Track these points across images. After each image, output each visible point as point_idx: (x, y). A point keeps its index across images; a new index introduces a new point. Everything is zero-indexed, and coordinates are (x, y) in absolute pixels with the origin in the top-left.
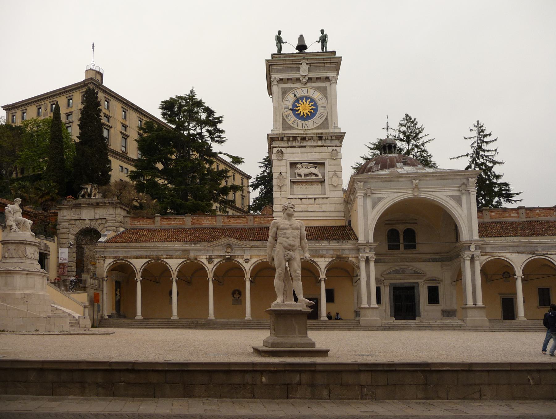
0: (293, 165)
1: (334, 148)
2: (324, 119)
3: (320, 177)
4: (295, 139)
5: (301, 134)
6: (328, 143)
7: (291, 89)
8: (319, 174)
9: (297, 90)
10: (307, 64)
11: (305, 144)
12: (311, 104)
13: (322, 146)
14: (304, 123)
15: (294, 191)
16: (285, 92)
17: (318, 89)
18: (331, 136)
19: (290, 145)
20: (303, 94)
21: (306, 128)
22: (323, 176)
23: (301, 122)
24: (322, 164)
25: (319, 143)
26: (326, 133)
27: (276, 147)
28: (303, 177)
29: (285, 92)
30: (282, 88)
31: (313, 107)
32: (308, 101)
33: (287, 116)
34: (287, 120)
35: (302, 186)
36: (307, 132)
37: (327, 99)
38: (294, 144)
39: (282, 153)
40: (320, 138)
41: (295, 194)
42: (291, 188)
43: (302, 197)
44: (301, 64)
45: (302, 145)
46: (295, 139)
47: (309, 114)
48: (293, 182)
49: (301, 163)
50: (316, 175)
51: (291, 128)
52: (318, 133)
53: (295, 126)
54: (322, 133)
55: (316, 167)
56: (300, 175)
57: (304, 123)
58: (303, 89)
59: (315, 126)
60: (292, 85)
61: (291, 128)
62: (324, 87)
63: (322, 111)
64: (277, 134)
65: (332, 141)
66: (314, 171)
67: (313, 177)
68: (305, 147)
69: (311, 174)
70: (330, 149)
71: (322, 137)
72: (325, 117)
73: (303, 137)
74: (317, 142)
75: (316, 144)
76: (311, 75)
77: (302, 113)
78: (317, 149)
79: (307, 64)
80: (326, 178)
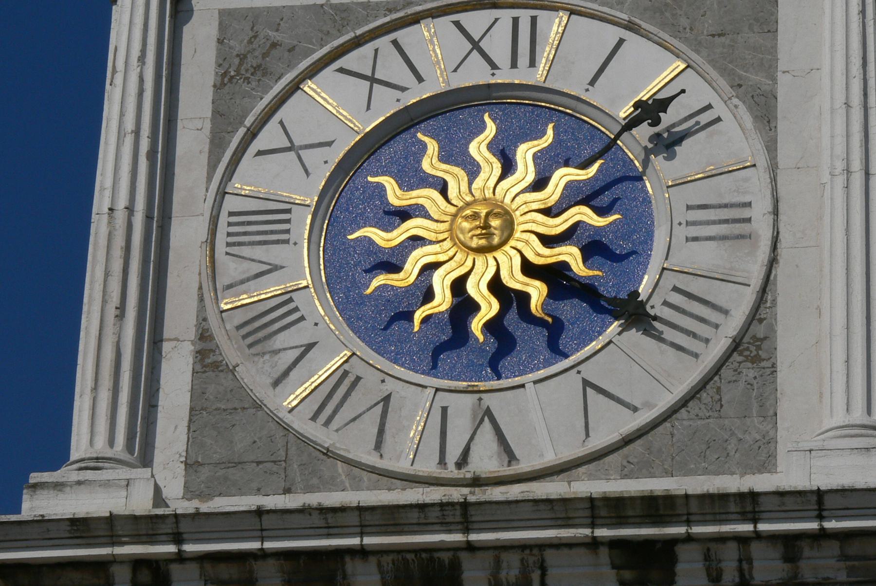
12: (563, 176)
14: (462, 407)
20: (476, 74)
26: (716, 505)
32: (525, 154)
33: (260, 328)
34: (254, 376)
37: (764, 110)
47: (537, 291)
52: (615, 508)
53: (357, 444)
54: (656, 508)
57: (462, 407)
59: (600, 439)
63: (707, 256)
72: (732, 326)
77: (441, 283)
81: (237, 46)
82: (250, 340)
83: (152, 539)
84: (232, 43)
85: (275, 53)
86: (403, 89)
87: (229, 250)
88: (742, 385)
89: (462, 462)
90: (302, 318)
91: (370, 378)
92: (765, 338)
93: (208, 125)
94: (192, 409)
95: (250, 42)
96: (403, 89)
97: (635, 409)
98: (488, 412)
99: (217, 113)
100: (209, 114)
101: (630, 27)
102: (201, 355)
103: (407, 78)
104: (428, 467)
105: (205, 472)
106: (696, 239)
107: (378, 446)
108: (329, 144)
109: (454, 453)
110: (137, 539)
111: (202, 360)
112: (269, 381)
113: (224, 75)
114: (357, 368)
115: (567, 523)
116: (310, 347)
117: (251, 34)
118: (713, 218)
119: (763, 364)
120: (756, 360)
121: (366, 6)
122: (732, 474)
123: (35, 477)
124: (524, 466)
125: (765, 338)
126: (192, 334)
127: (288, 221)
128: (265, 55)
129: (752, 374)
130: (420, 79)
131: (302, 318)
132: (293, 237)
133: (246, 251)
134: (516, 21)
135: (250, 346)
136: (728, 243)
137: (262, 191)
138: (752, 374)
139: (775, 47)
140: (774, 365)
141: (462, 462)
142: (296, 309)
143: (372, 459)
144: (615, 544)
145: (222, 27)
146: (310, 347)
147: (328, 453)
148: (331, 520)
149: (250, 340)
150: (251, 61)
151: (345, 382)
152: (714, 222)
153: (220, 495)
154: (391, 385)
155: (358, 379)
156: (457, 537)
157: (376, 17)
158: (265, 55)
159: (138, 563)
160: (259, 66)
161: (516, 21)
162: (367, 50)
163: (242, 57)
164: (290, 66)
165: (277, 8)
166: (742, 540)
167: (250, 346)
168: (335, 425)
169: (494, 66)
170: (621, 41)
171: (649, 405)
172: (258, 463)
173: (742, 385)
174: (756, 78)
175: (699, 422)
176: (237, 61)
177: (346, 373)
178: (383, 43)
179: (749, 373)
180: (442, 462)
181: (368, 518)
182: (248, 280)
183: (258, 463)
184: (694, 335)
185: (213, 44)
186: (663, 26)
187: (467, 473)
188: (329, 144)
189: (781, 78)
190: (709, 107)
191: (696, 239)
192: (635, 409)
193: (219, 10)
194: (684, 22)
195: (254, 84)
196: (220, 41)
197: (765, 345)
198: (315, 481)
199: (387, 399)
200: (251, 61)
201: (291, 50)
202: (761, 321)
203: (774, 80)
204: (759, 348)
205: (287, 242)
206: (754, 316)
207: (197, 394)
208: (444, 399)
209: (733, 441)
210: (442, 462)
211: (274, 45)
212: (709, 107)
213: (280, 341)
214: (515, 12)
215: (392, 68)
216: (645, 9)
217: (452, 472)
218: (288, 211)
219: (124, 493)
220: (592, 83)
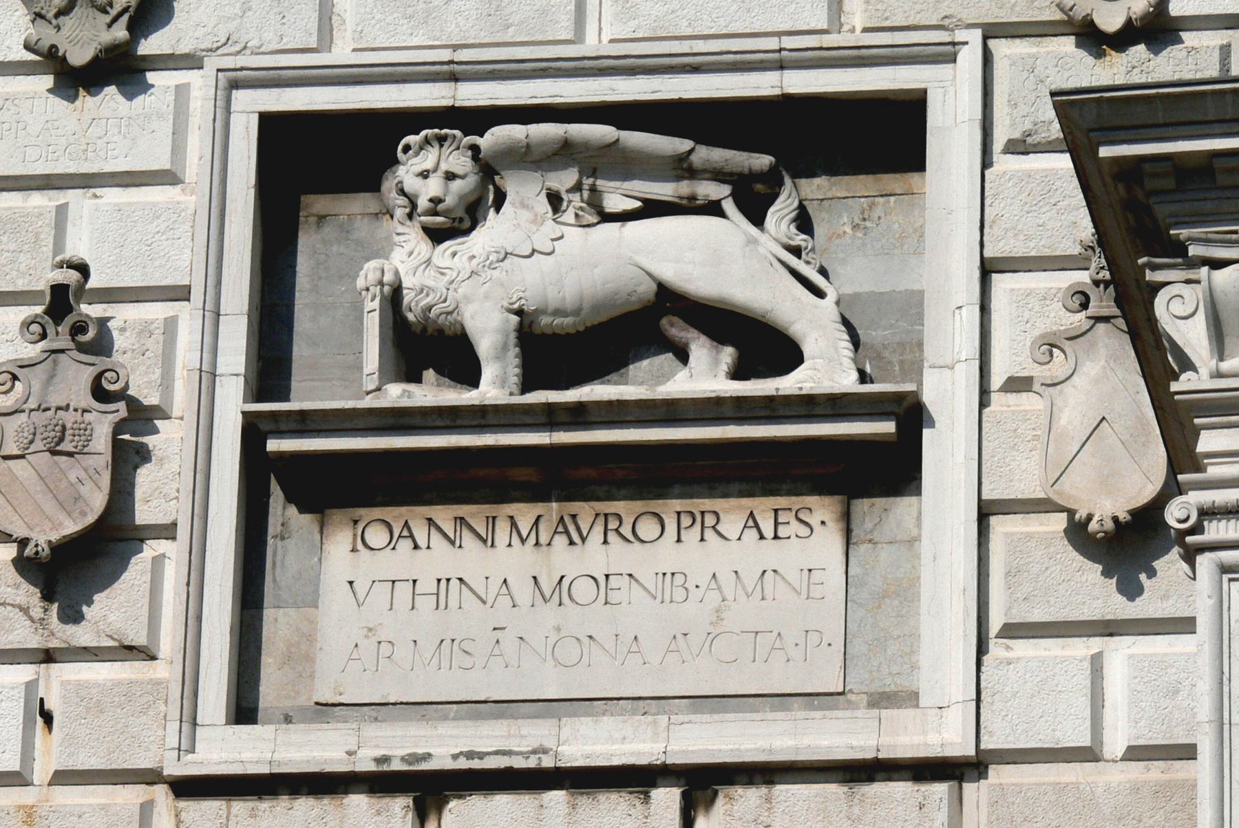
0: (318, 162)
3: (826, 368)
8: (814, 325)
15: (303, 657)
24: (885, 137)
35: (469, 560)
41: (325, 710)
43: (442, 746)
48: (307, 478)
50: (762, 345)
69: (654, 320)
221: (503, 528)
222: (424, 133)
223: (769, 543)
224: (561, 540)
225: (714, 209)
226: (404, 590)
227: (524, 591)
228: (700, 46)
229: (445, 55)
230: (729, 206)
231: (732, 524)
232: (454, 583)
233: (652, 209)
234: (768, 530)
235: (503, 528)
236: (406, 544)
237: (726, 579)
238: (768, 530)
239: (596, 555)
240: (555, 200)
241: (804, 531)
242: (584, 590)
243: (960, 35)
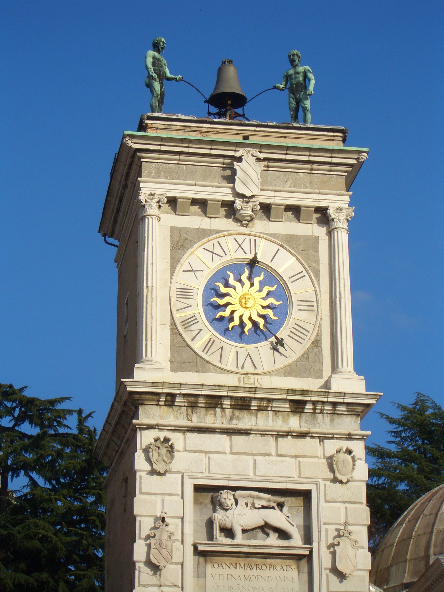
1: (345, 444)
2: (307, 343)
4: (214, 402)
5: (236, 389)
6: (323, 424)
7: (203, 233)
9: (222, 240)
10: (258, 159)
11: (245, 421)
12: (267, 289)
13: (302, 435)
16: (181, 243)
17: (289, 242)
18: (335, 404)
19: (196, 421)
21: (249, 368)
22: (308, 538)
23: (232, 348)
25: (294, 423)
27: (150, 427)
28: (239, 538)
29: (181, 243)
30: (173, 229)
31: (271, 300)
33: (188, 323)
34: (187, 337)
35: (232, 571)
36: (253, 381)
38: (211, 420)
39: (171, 449)
40: (298, 407)
42: (200, 574)
44: (239, 160)
45: (235, 424)
46: (214, 402)
49: (234, 489)
50: (284, 535)
51: (198, 363)
52: (294, 392)
53: (214, 359)
54: (303, 392)
55: (281, 506)
56: (229, 532)
58: (240, 238)
60: (204, 223)
61: (198, 363)
62: (306, 238)
64: (154, 384)
65: (337, 419)
66: (277, 518)
67: (273, 540)
68: (247, 433)
70: (331, 447)
71: (304, 403)
73: (243, 399)
74: (285, 420)
75: (280, 425)
76: (267, 197)
78: (288, 444)
79: (258, 159)
80: (315, 546)
81: (176, 239)
82: (185, 326)
83: (173, 388)
84: (174, 237)
85: (187, 241)
86: (221, 257)
87: (177, 299)
88: (314, 353)
89: (242, 367)
90: (198, 322)
91: (217, 341)
92: (319, 341)
93: (169, 261)
94: (171, 346)
95: (179, 237)
96: (221, 257)
97: (287, 357)
98: (249, 354)
99: (172, 258)
100: (170, 258)
101: (281, 246)
102: (172, 329)
103: (222, 254)
104: (234, 369)
105: (175, 364)
106: (300, 310)
107: (220, 361)
108: (202, 271)
109: (240, 365)
110: (169, 388)
111: (172, 331)
112: (191, 339)
113: (173, 246)
114: (214, 338)
115: (281, 394)
116: (201, 330)
117: (179, 235)
118: (304, 304)
119: (319, 348)
120: (317, 346)
121: (210, 230)
122: (312, 378)
123: (136, 365)
124: (259, 370)
125: (319, 341)
126: (169, 323)
127: (193, 292)
128: (184, 242)
129: (316, 350)
130: (226, 254)
131: (198, 322)
132: (194, 297)
133: (182, 300)
134: (250, 240)
135: (185, 328)
136: (309, 312)
137: (185, 283)
138: (316, 350)
139: (318, 257)
140: (322, 349)
141: (242, 367)
142: (196, 319)
143: (219, 365)
144: (291, 401)
145: (171, 232)
146: (201, 330)
147: (208, 362)
148: (221, 388)
149: (185, 326)
150: (180, 243)
151: (210, 342)
152: (305, 306)
153: (180, 371)
154: (223, 344)
155: (214, 341)
156: (252, 395)
157: (213, 234)
158: (184, 242)
159: (168, 394)
160: (182, 245)
161: (250, 240)
162: (211, 243)
163: (178, 242)
164: (191, 246)
165: (186, 228)
166: (323, 403)
167: (185, 328)
168: (209, 353)
169: (245, 253)
170: (279, 249)
171: (291, 357)
172: (189, 363)
173: (314, 353)
174: (314, 265)
175: (303, 363)
176: (176, 243)
177: (211, 339)
178: (215, 241)
179: (316, 350)
180: (237, 367)
181: (230, 388)
182: (183, 309)
183: (189, 363)
184: (301, 338)
185: (169, 237)
186: (289, 246)
187: (244, 371)
188: (202, 271)
189: (321, 266)
190: (302, 272)
191: (300, 310)
192: (287, 357)
193: (171, 227)
194: (295, 246)
195: (181, 250)
196: (171, 236)
197: (319, 342)
198: (205, 369)
199: (222, 348)
200: (180, 243)
201: (191, 241)
202: (318, 335)
203: (319, 266)
204: (318, 343)
205: (193, 298)
206: (317, 335)
207: (172, 341)
208: (238, 349)
209: (312, 369)
210: (237, 367)
211: (186, 239)
212: (302, 272)
213: (193, 327)
214: (251, 237)
215: (217, 250)
216: (285, 241)
217: (240, 371)
218: (193, 289)
219: (161, 373)
220: (271, 261)
221: (238, 565)
222: (225, 491)
223: (285, 572)
224: (249, 569)
225: (273, 508)
226: (221, 576)
227: (243, 578)
228: (273, 478)
229: (228, 476)
230: (276, 507)
231: (279, 568)
232: (230, 575)
233: (263, 507)
234: (285, 569)
235: (238, 565)
236: (221, 567)
237: (278, 578)
238: (285, 569)
239: (255, 572)
240: (247, 504)
241: (291, 569)
242: (253, 578)
243: (318, 480)
